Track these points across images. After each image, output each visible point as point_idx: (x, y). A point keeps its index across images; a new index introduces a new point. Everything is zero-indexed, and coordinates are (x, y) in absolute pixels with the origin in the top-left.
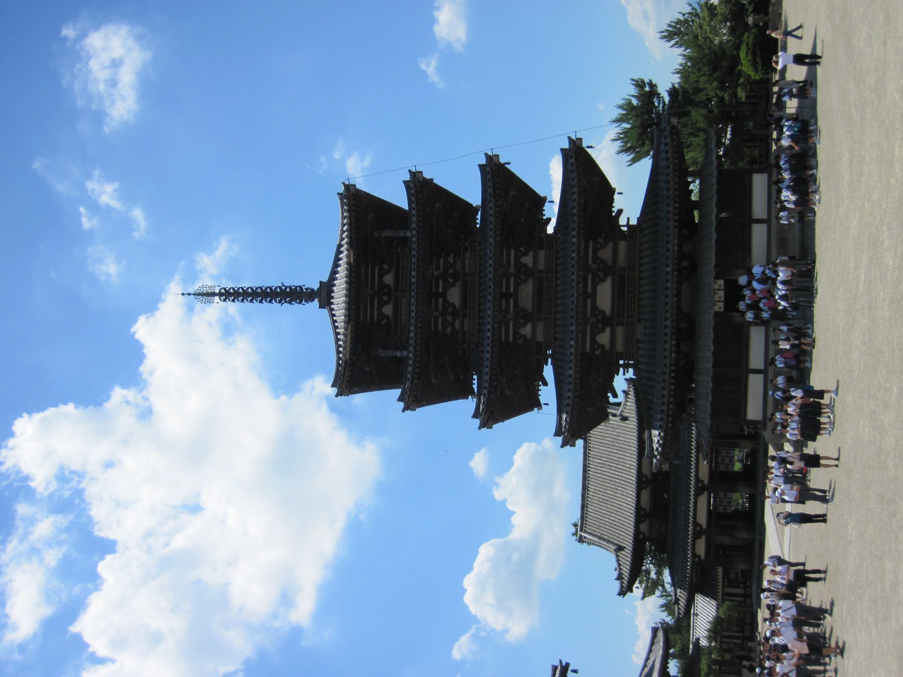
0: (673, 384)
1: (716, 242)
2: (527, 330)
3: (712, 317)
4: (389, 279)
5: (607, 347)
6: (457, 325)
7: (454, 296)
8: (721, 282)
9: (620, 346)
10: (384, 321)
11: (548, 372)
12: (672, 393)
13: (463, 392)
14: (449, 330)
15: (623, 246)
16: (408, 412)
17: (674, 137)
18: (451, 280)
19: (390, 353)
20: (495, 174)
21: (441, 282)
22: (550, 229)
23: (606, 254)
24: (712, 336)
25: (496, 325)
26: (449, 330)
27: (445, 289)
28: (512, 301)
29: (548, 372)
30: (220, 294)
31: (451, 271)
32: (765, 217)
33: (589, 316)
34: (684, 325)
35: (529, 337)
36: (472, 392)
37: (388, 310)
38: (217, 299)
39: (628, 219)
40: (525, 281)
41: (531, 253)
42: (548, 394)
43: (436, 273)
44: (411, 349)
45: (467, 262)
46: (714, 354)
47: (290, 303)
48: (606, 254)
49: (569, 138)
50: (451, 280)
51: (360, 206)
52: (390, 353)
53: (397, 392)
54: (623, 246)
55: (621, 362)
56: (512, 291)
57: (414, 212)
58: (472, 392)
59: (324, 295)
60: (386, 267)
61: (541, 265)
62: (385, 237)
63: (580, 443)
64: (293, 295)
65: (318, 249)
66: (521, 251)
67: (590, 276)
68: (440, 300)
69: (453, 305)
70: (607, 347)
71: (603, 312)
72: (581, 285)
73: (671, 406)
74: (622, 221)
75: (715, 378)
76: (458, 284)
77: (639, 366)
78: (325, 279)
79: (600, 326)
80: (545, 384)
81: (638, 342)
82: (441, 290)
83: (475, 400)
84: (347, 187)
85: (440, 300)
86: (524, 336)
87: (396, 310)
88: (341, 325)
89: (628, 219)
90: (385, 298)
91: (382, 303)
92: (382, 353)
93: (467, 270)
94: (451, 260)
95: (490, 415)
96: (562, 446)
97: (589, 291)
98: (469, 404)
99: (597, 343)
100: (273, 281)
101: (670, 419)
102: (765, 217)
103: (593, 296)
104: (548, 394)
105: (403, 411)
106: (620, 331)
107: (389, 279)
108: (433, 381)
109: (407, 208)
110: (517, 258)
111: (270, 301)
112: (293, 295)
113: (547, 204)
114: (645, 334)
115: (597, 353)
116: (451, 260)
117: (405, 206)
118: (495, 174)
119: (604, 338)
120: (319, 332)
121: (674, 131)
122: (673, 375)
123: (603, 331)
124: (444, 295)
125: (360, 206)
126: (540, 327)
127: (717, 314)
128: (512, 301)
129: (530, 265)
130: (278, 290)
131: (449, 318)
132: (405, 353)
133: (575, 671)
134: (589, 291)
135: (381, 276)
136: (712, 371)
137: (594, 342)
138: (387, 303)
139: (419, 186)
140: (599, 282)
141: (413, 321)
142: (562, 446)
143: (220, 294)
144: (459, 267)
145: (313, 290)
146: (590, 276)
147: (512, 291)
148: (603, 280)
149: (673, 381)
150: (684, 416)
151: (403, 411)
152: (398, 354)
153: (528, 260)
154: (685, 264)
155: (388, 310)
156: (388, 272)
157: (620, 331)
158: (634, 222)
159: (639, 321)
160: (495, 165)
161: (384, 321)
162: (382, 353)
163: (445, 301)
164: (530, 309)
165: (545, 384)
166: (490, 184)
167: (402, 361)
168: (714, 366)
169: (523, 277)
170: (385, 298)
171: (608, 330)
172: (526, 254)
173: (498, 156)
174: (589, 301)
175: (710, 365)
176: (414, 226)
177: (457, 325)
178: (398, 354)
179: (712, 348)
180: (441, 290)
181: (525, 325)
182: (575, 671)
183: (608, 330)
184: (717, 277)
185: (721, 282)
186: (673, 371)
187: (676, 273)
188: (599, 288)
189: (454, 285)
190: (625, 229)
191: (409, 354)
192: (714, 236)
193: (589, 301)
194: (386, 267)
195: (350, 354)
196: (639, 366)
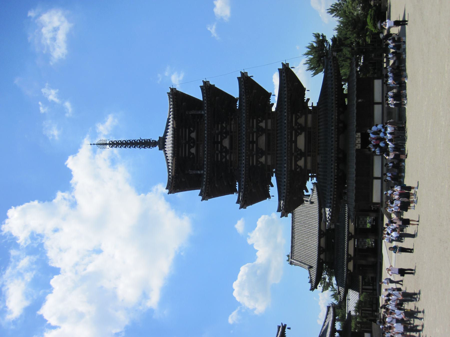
0: (336, 185)
1: (356, 114)
2: (263, 160)
3: (355, 151)
4: (193, 135)
5: (303, 167)
7: (226, 143)
8: (359, 134)
9: (309, 167)
10: (192, 156)
11: (274, 180)
12: (335, 190)
13: (231, 191)
14: (224, 160)
15: (310, 116)
16: (204, 201)
17: (335, 62)
18: (224, 135)
19: (194, 172)
20: (246, 82)
21: (219, 136)
22: (273, 109)
23: (301, 121)
24: (355, 161)
25: (247, 157)
26: (224, 160)
27: (222, 140)
28: (255, 145)
29: (274, 180)
31: (224, 131)
32: (381, 101)
33: (293, 152)
34: (341, 156)
35: (264, 163)
36: (235, 191)
39: (312, 103)
40: (261, 135)
41: (264, 121)
42: (274, 191)
43: (217, 132)
44: (205, 170)
45: (232, 126)
46: (356, 170)
47: (144, 148)
48: (301, 121)
49: (282, 63)
50: (224, 135)
51: (179, 99)
52: (194, 172)
53: (199, 191)
54: (310, 116)
55: (310, 175)
56: (255, 140)
57: (205, 102)
58: (235, 191)
59: (161, 143)
60: (192, 129)
61: (269, 127)
62: (192, 115)
63: (290, 215)
64: (146, 144)
65: (158, 121)
66: (259, 120)
67: (294, 132)
68: (219, 145)
69: (226, 147)
70: (303, 167)
71: (300, 150)
72: (289, 137)
73: (335, 196)
74: (309, 104)
75: (357, 182)
76: (228, 137)
77: (319, 176)
78: (162, 136)
79: (299, 157)
80: (272, 186)
81: (318, 164)
82: (219, 140)
83: (237, 195)
84: (172, 89)
85: (219, 145)
86: (261, 163)
87: (197, 151)
88: (170, 158)
89: (312, 103)
90: (192, 145)
91: (190, 147)
92: (191, 172)
93: (232, 130)
94: (224, 125)
95: (245, 202)
96: (281, 217)
97: (293, 139)
98: (234, 197)
99: (298, 165)
100: (136, 137)
101: (335, 202)
102: (381, 101)
103: (296, 142)
104: (274, 191)
105: (202, 200)
106: (309, 159)
107: (193, 135)
108: (216, 185)
109: (202, 99)
110: (257, 123)
111: (135, 147)
112: (146, 144)
113: (272, 96)
114: (321, 161)
115: (298, 170)
116: (224, 125)
117: (202, 99)
118: (246, 82)
120: (159, 162)
121: (334, 59)
122: (336, 180)
123: (300, 159)
124: (221, 143)
125: (179, 99)
126: (269, 157)
127: (357, 150)
128: (255, 145)
129: (264, 127)
130: (138, 141)
131: (224, 154)
132: (202, 172)
133: (289, 328)
134: (293, 139)
135: (190, 133)
136: (355, 179)
137: (296, 165)
138: (193, 147)
139: (208, 89)
140: (298, 135)
141: (206, 156)
142: (281, 217)
144: (228, 128)
146: (294, 132)
147: (255, 140)
148: (300, 134)
149: (336, 184)
150: (342, 201)
151: (202, 200)
152: (199, 172)
153: (263, 125)
154: (341, 125)
155: (193, 150)
156: (193, 132)
157: (309, 159)
158: (315, 105)
160: (246, 77)
161: (192, 156)
162: (191, 172)
163: (222, 145)
164: (264, 149)
165: (272, 186)
166: (243, 87)
167: (201, 175)
168: (356, 176)
169: (260, 133)
170: (192, 145)
171: (303, 159)
172: (261, 121)
173: (247, 73)
174: (293, 144)
175: (354, 175)
176: (205, 108)
178: (199, 172)
179: (355, 167)
180: (219, 140)
181: (262, 157)
182: (289, 328)
183: (303, 159)
184: (357, 132)
185: (359, 134)
186: (335, 179)
187: (336, 130)
188: (298, 138)
189: (225, 138)
190: (311, 108)
191: (204, 172)
192: (355, 111)
193: (293, 144)
194: (192, 129)
195: (175, 173)
196: (319, 176)
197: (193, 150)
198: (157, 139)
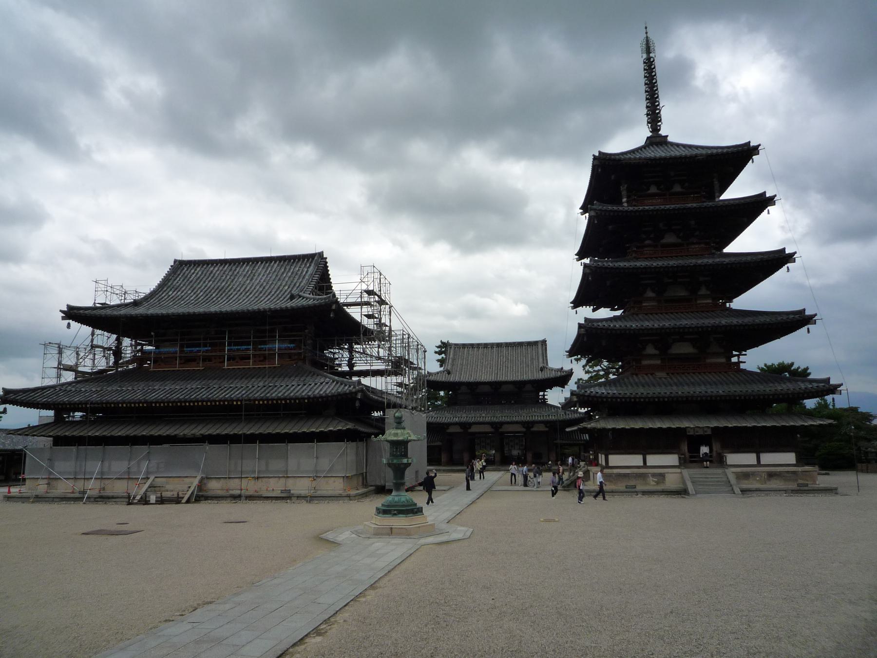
2: (650, 294)
5: (645, 353)
6: (647, 242)
7: (670, 239)
18: (681, 234)
19: (624, 193)
24: (664, 427)
30: (649, 58)
37: (653, 190)
38: (645, 56)
52: (624, 193)
54: (723, 360)
59: (658, 140)
70: (645, 353)
78: (670, 139)
80: (594, 310)
87: (653, 195)
88: (638, 156)
106: (659, 362)
107: (677, 188)
108: (610, 227)
116: (697, 233)
119: (650, 350)
120: (628, 139)
131: (652, 236)
132: (625, 204)
143: (649, 58)
145: (659, 130)
152: (624, 200)
153: (703, 291)
159: (668, 374)
165: (594, 310)
167: (620, 203)
177: (647, 242)
178: (624, 200)
183: (657, 352)
191: (625, 206)
194: (687, 184)
197: (653, 190)
198: (663, 132)
